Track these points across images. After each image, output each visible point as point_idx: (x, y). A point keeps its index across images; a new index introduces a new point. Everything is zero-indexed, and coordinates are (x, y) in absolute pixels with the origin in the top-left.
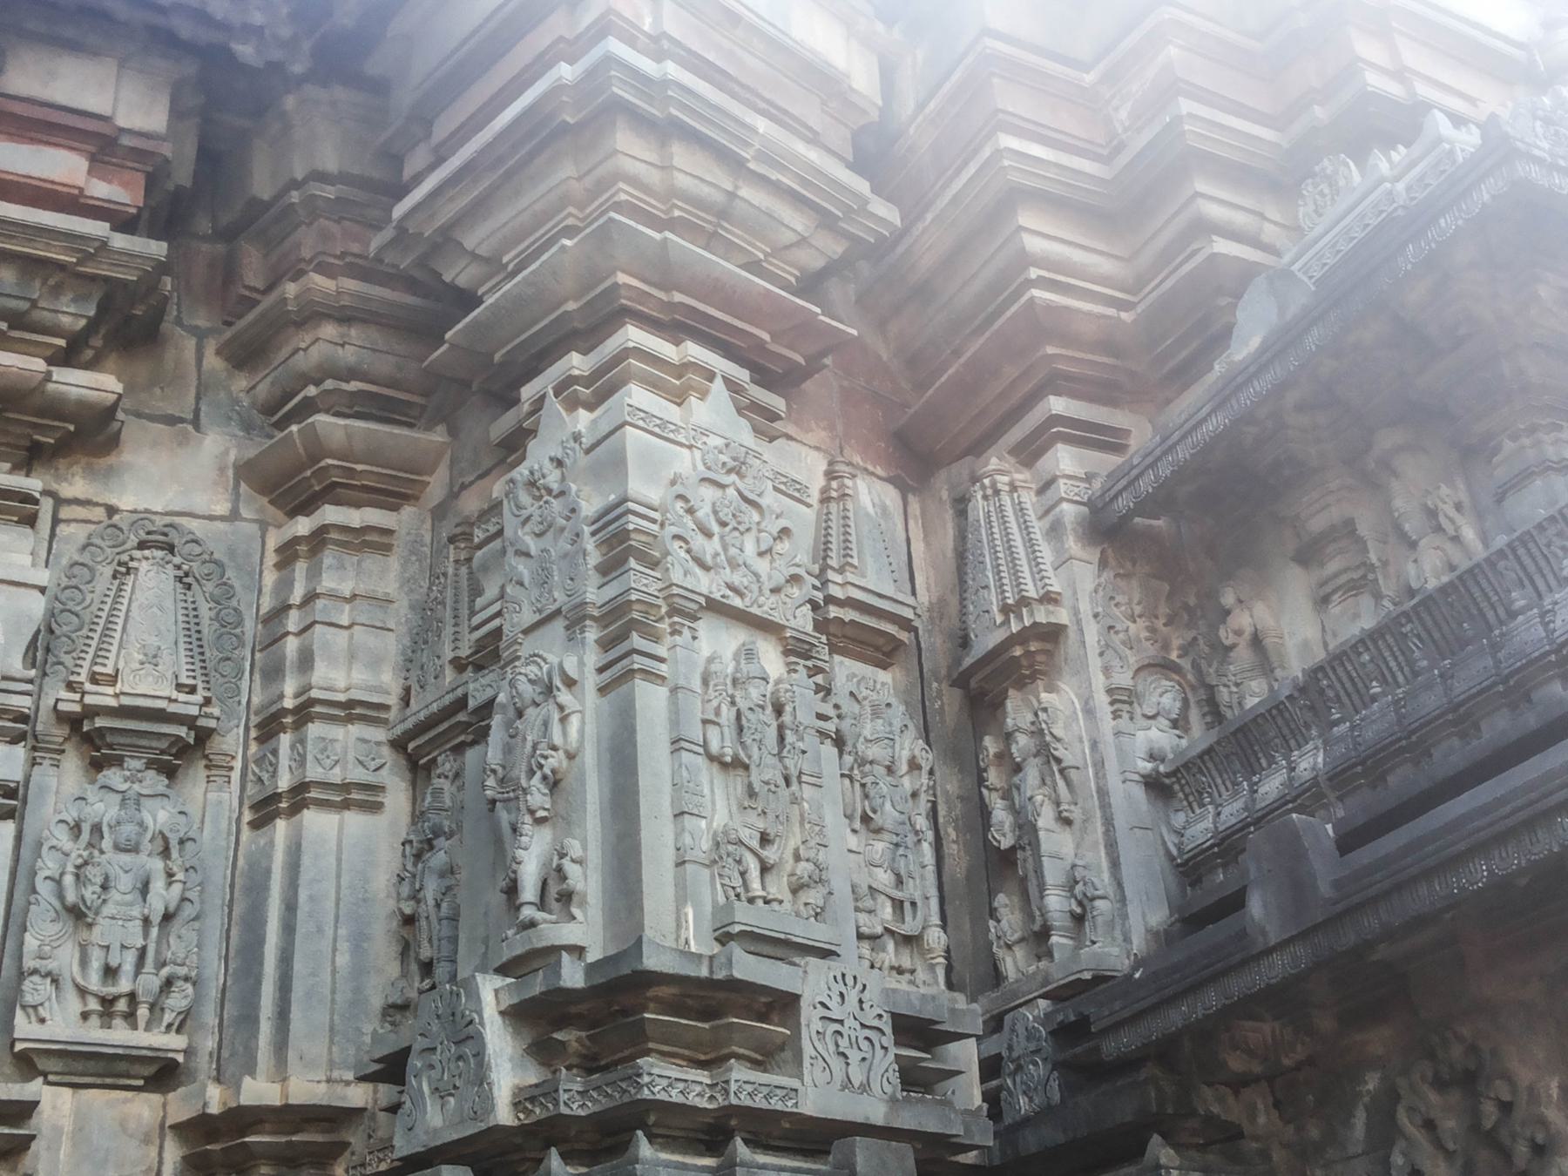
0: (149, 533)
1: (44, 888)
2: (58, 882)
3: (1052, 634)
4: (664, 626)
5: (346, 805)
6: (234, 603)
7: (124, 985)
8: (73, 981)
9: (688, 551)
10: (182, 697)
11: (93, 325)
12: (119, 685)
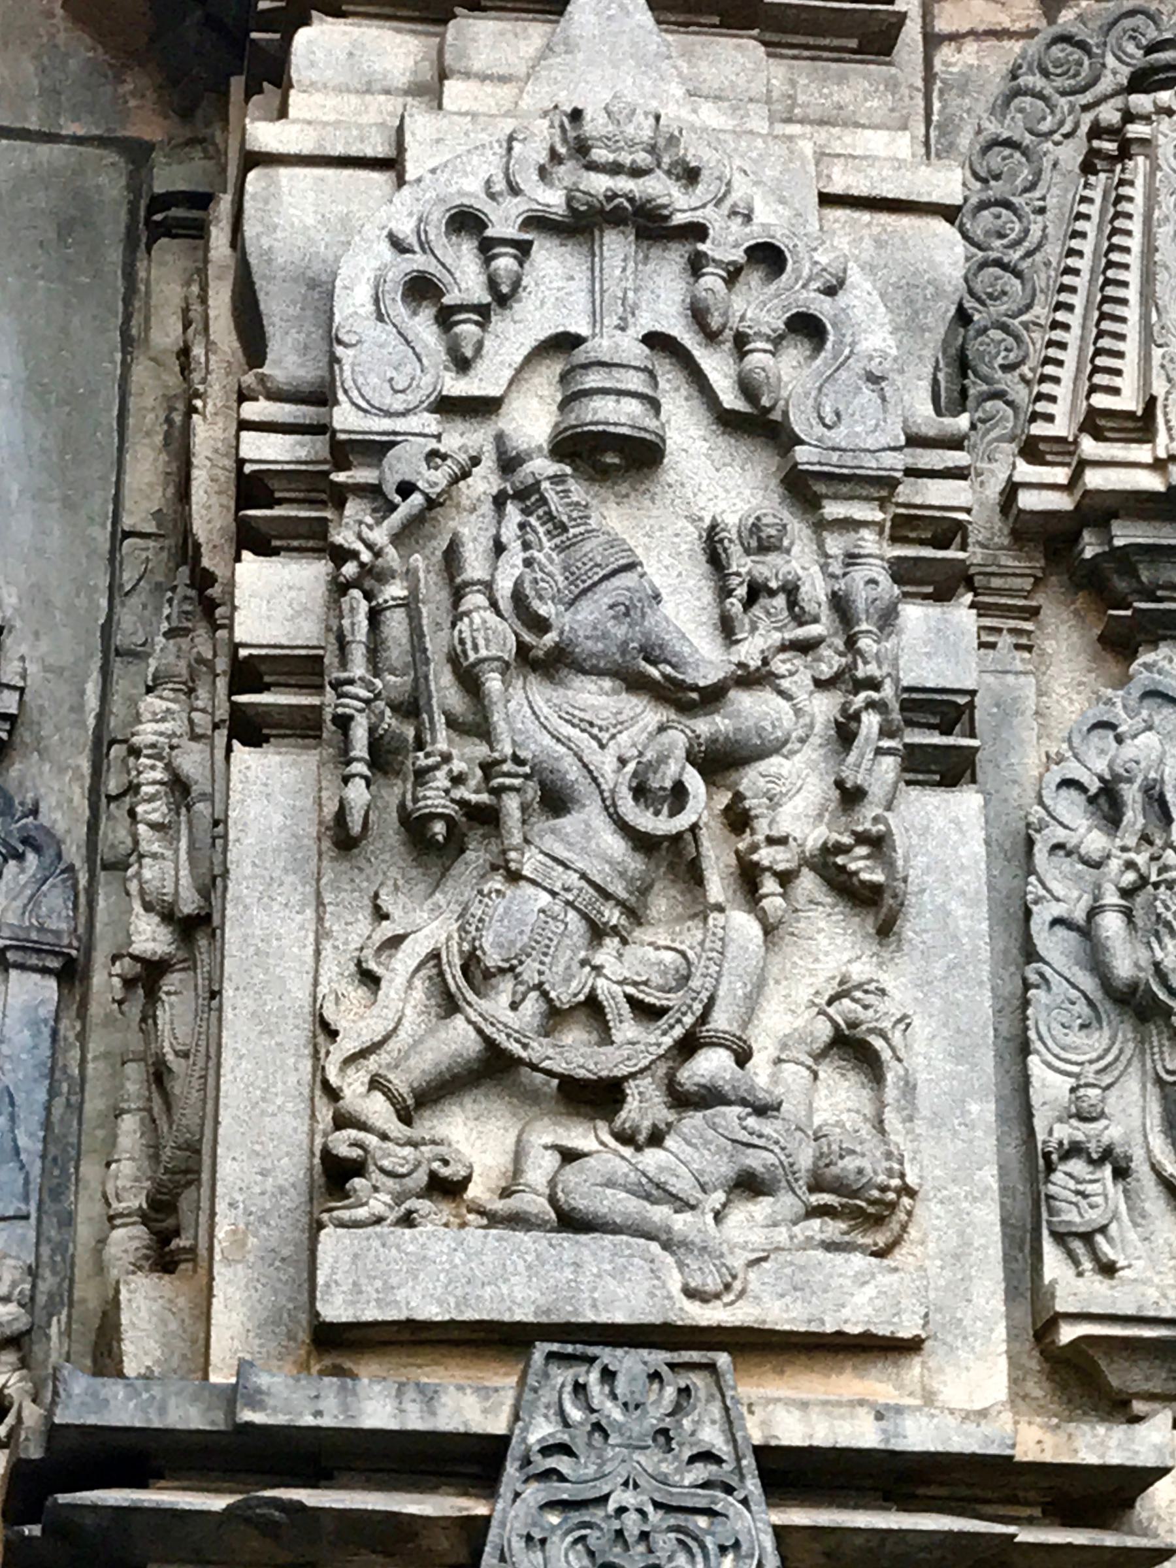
0: (1150, 49)
2: (1086, 930)
8: (1156, 1170)
12: (1162, 437)
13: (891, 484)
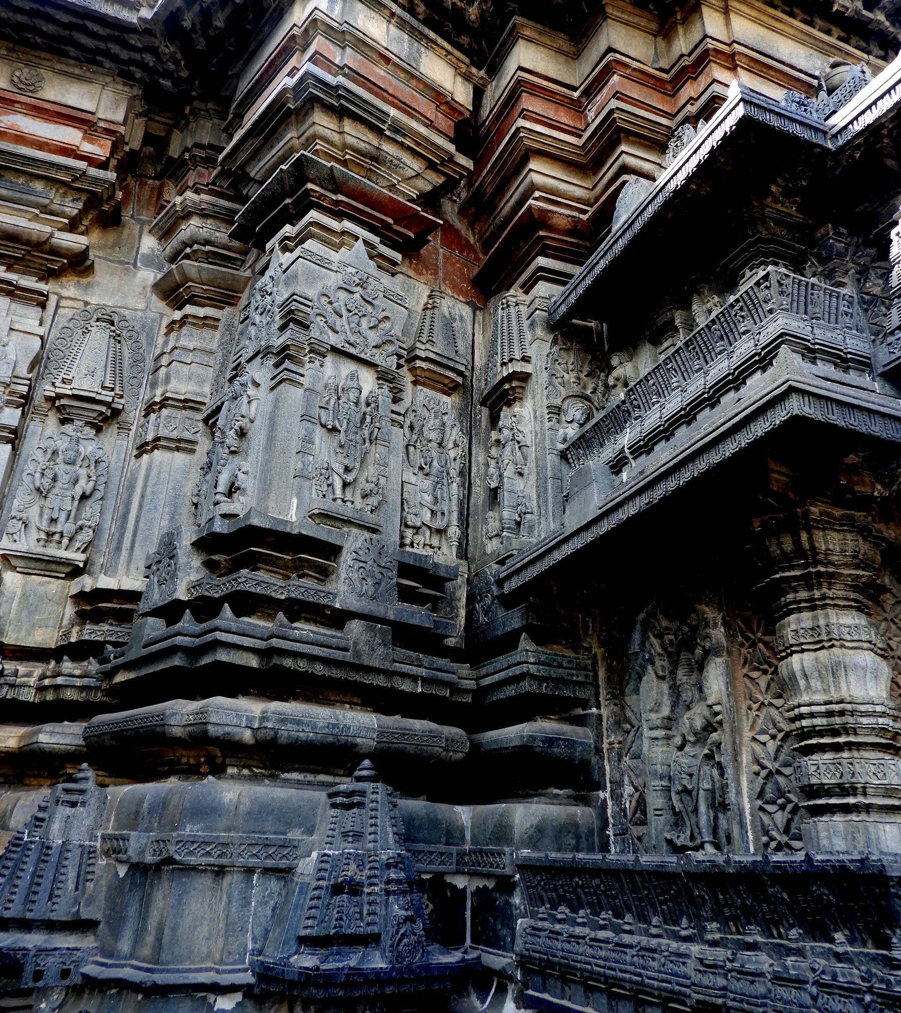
1: (27, 480)
3: (525, 377)
4: (307, 359)
5: (178, 449)
6: (141, 351)
7: (58, 528)
9: (326, 322)
10: (104, 392)
11: (82, 213)
13: (9, 385)
